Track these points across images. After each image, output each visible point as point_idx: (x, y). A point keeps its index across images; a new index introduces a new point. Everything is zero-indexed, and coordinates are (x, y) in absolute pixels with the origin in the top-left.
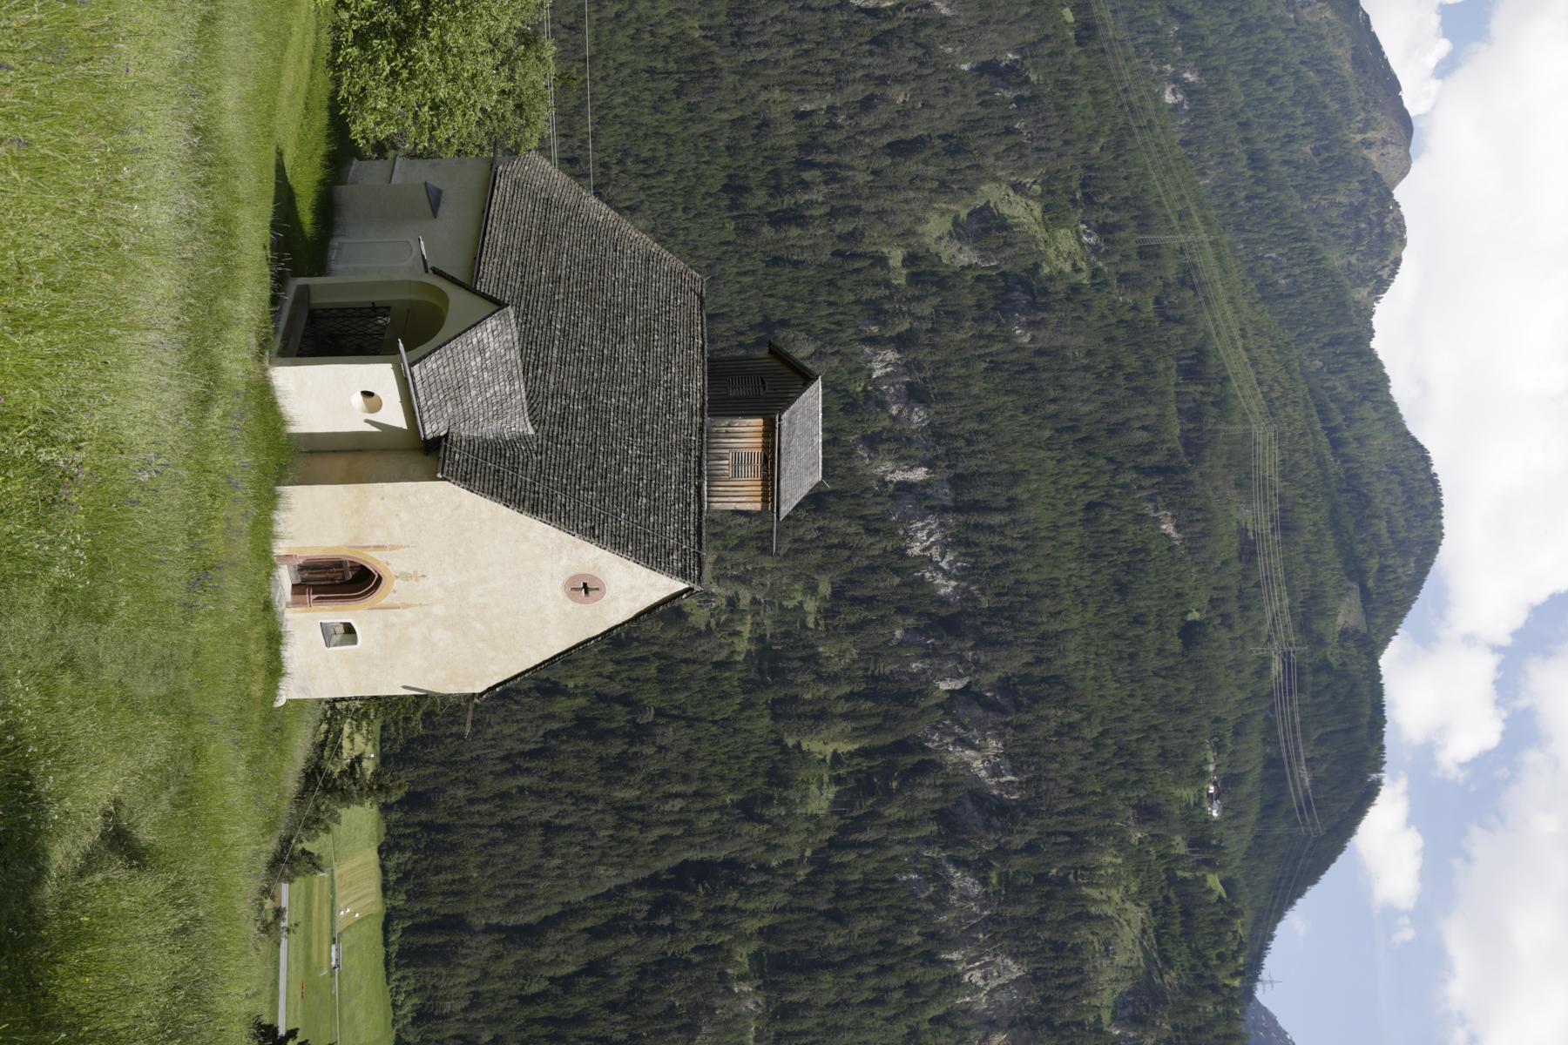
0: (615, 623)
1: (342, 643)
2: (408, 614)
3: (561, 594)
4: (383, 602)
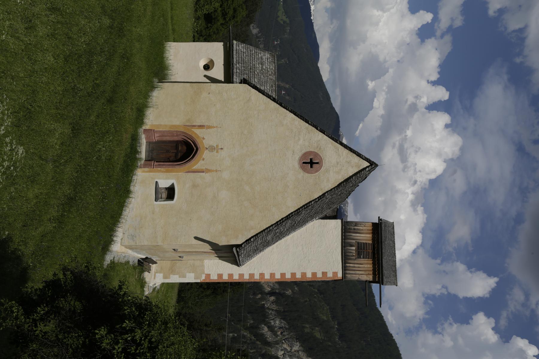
0: (326, 190)
1: (164, 201)
2: (207, 176)
3: (297, 165)
4: (195, 168)
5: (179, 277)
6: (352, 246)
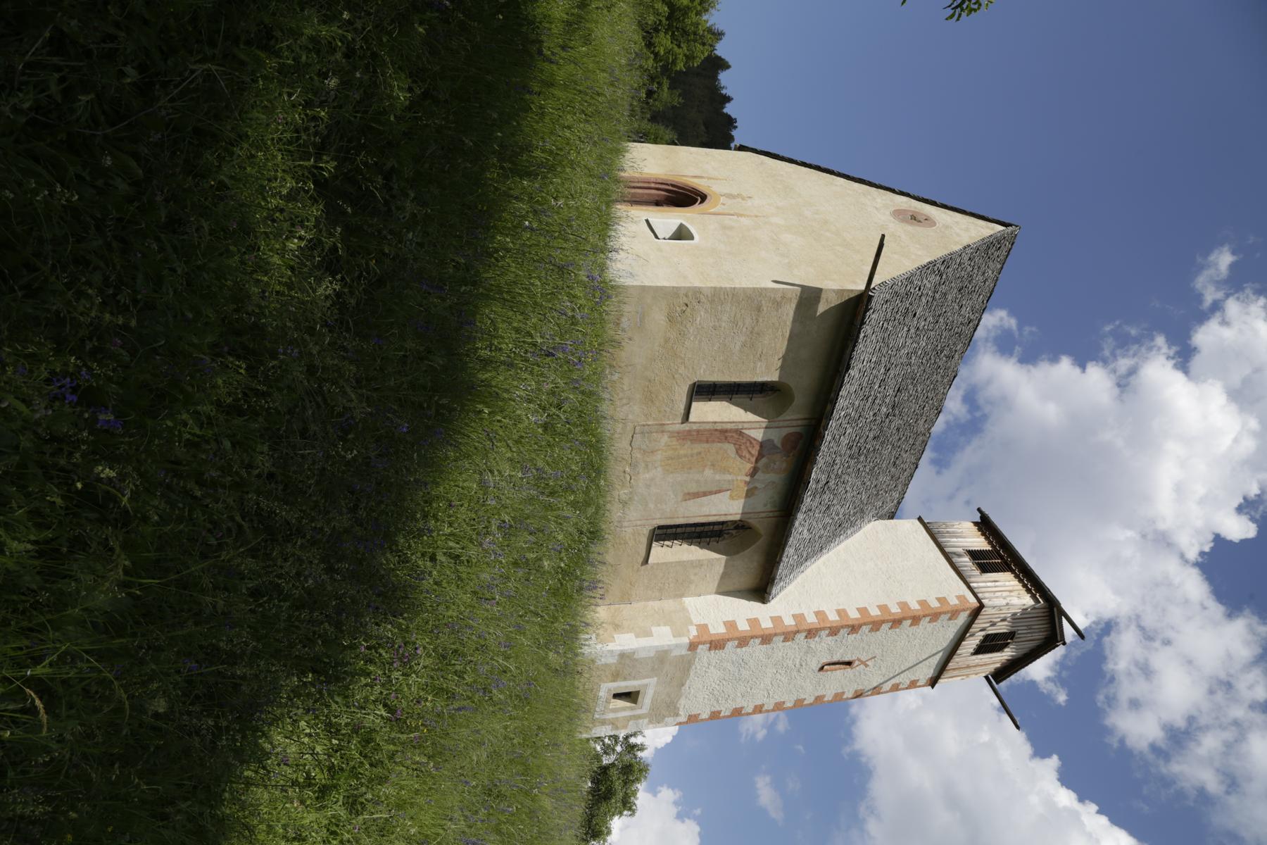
5: (637, 636)
6: (959, 555)
